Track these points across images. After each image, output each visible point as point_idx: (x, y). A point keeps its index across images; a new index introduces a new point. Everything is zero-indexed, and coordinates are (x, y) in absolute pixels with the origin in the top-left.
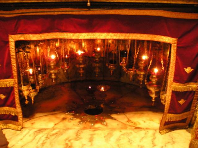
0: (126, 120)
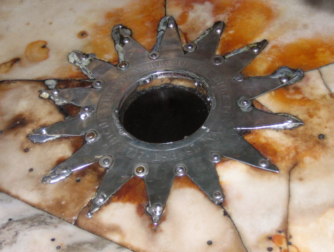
0: (271, 224)
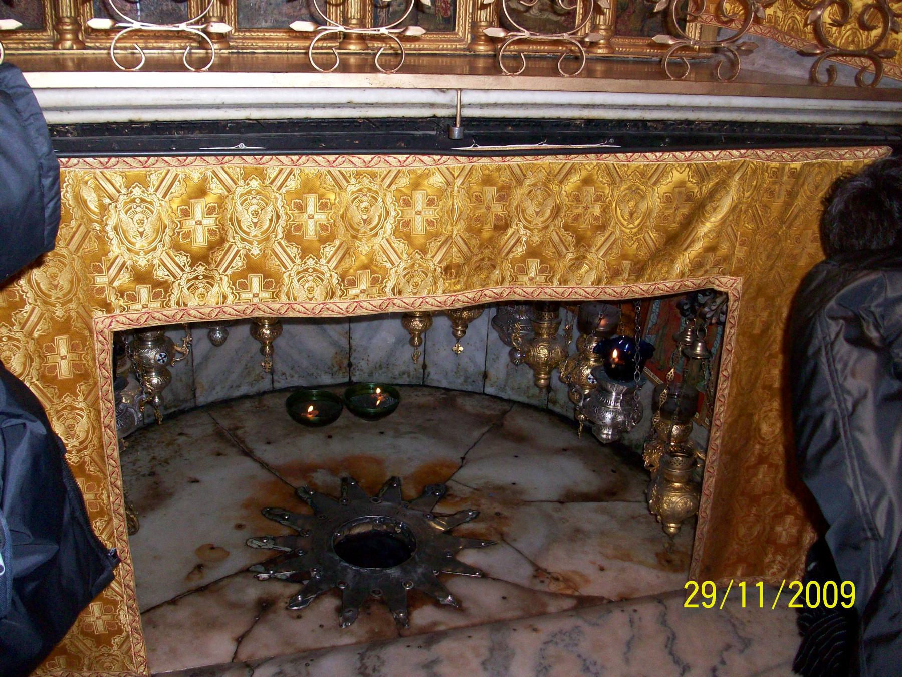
0: (528, 570)
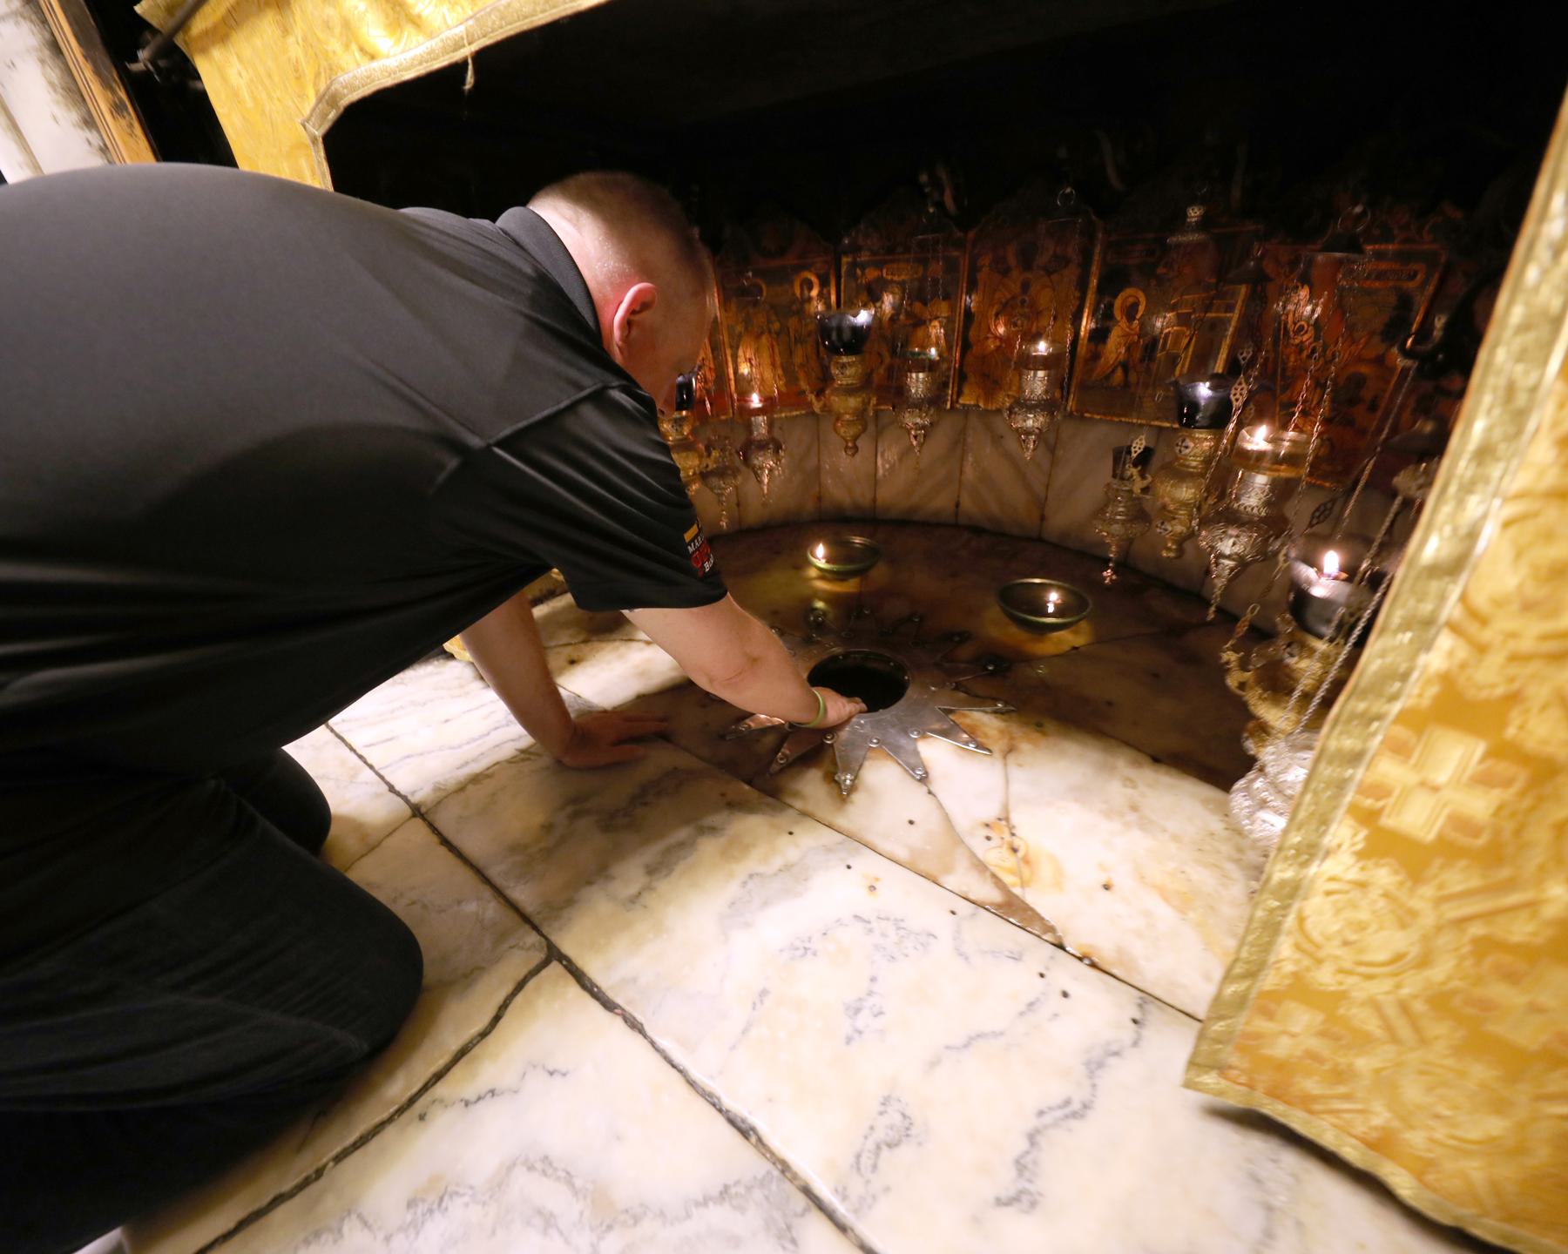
0: (991, 811)
